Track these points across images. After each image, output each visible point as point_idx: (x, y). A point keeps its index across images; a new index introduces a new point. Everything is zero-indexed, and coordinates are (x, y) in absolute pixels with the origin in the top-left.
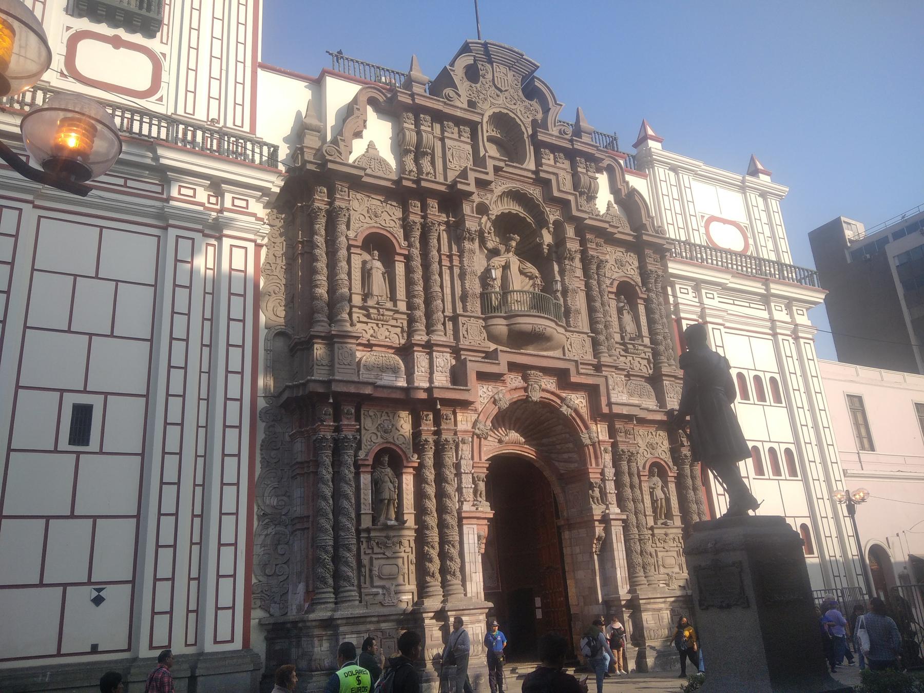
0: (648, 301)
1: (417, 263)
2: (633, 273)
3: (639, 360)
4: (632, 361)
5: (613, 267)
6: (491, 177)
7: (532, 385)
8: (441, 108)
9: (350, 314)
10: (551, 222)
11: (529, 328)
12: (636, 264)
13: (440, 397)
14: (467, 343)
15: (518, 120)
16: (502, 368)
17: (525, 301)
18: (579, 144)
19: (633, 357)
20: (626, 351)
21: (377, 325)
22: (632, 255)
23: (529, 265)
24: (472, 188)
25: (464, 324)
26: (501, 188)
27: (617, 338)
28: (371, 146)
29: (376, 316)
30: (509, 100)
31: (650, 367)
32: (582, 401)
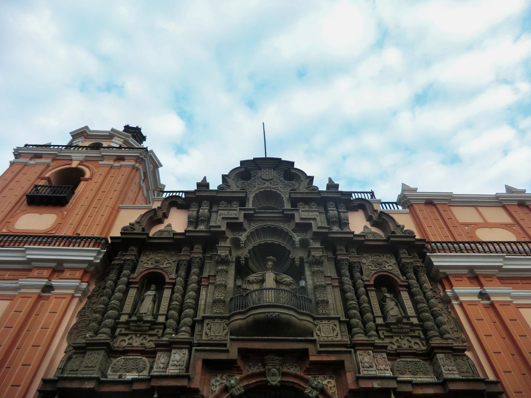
0: (409, 288)
1: (179, 287)
2: (391, 268)
3: (410, 338)
4: (400, 340)
5: (370, 267)
6: (241, 220)
7: (269, 370)
8: (215, 194)
9: (113, 329)
10: (297, 240)
11: (263, 316)
12: (394, 261)
13: (157, 385)
14: (210, 338)
15: (278, 192)
16: (233, 354)
17: (268, 297)
18: (325, 193)
19: (400, 337)
20: (390, 331)
21: (136, 336)
22: (389, 256)
23: (285, 275)
24: (224, 228)
25: (209, 324)
26: (253, 227)
27: (380, 321)
28: (169, 225)
29: (134, 328)
30: (273, 184)
31: (423, 344)
32: (331, 380)
